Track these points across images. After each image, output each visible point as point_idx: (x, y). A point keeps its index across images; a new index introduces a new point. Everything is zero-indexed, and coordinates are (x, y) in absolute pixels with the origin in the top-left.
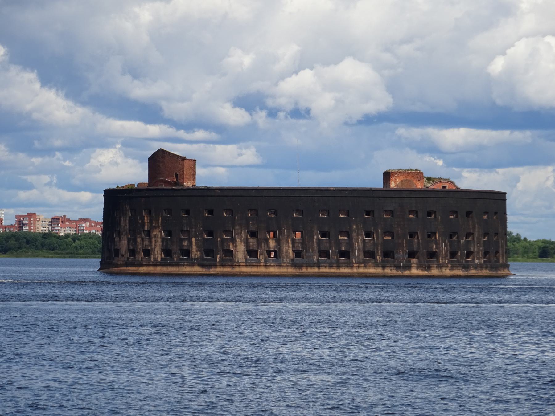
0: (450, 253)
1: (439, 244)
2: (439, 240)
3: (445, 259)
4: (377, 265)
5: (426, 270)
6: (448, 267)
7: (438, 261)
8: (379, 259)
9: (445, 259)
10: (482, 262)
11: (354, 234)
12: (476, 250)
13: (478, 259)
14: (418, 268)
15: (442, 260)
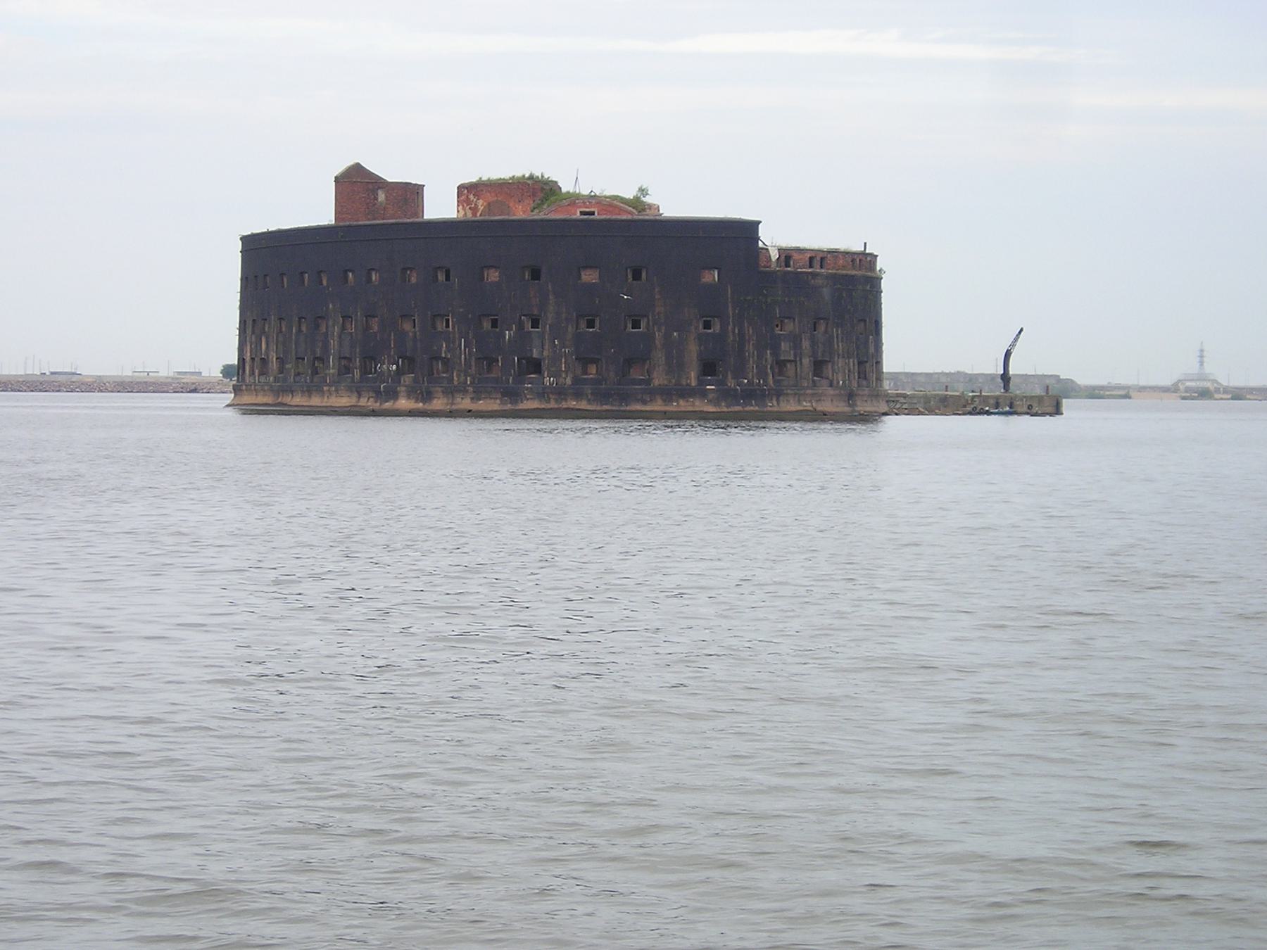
0: (478, 359)
1: (454, 342)
2: (454, 332)
3: (466, 376)
4: (349, 389)
5: (424, 401)
6: (465, 391)
7: (451, 380)
8: (357, 374)
9: (466, 376)
10: (569, 381)
11: (330, 323)
12: (546, 353)
13: (556, 375)
14: (411, 394)
15: (458, 376)
